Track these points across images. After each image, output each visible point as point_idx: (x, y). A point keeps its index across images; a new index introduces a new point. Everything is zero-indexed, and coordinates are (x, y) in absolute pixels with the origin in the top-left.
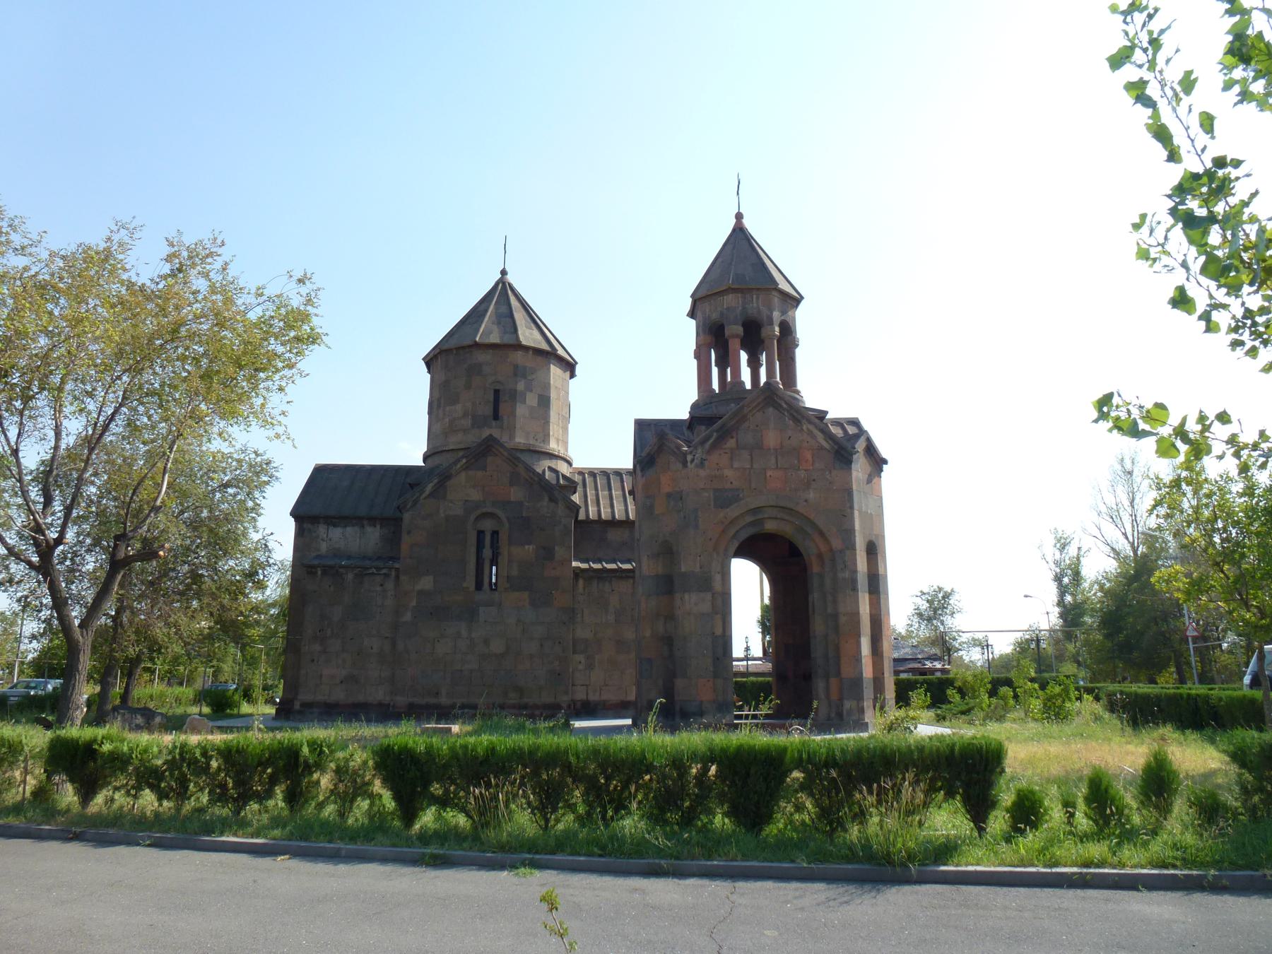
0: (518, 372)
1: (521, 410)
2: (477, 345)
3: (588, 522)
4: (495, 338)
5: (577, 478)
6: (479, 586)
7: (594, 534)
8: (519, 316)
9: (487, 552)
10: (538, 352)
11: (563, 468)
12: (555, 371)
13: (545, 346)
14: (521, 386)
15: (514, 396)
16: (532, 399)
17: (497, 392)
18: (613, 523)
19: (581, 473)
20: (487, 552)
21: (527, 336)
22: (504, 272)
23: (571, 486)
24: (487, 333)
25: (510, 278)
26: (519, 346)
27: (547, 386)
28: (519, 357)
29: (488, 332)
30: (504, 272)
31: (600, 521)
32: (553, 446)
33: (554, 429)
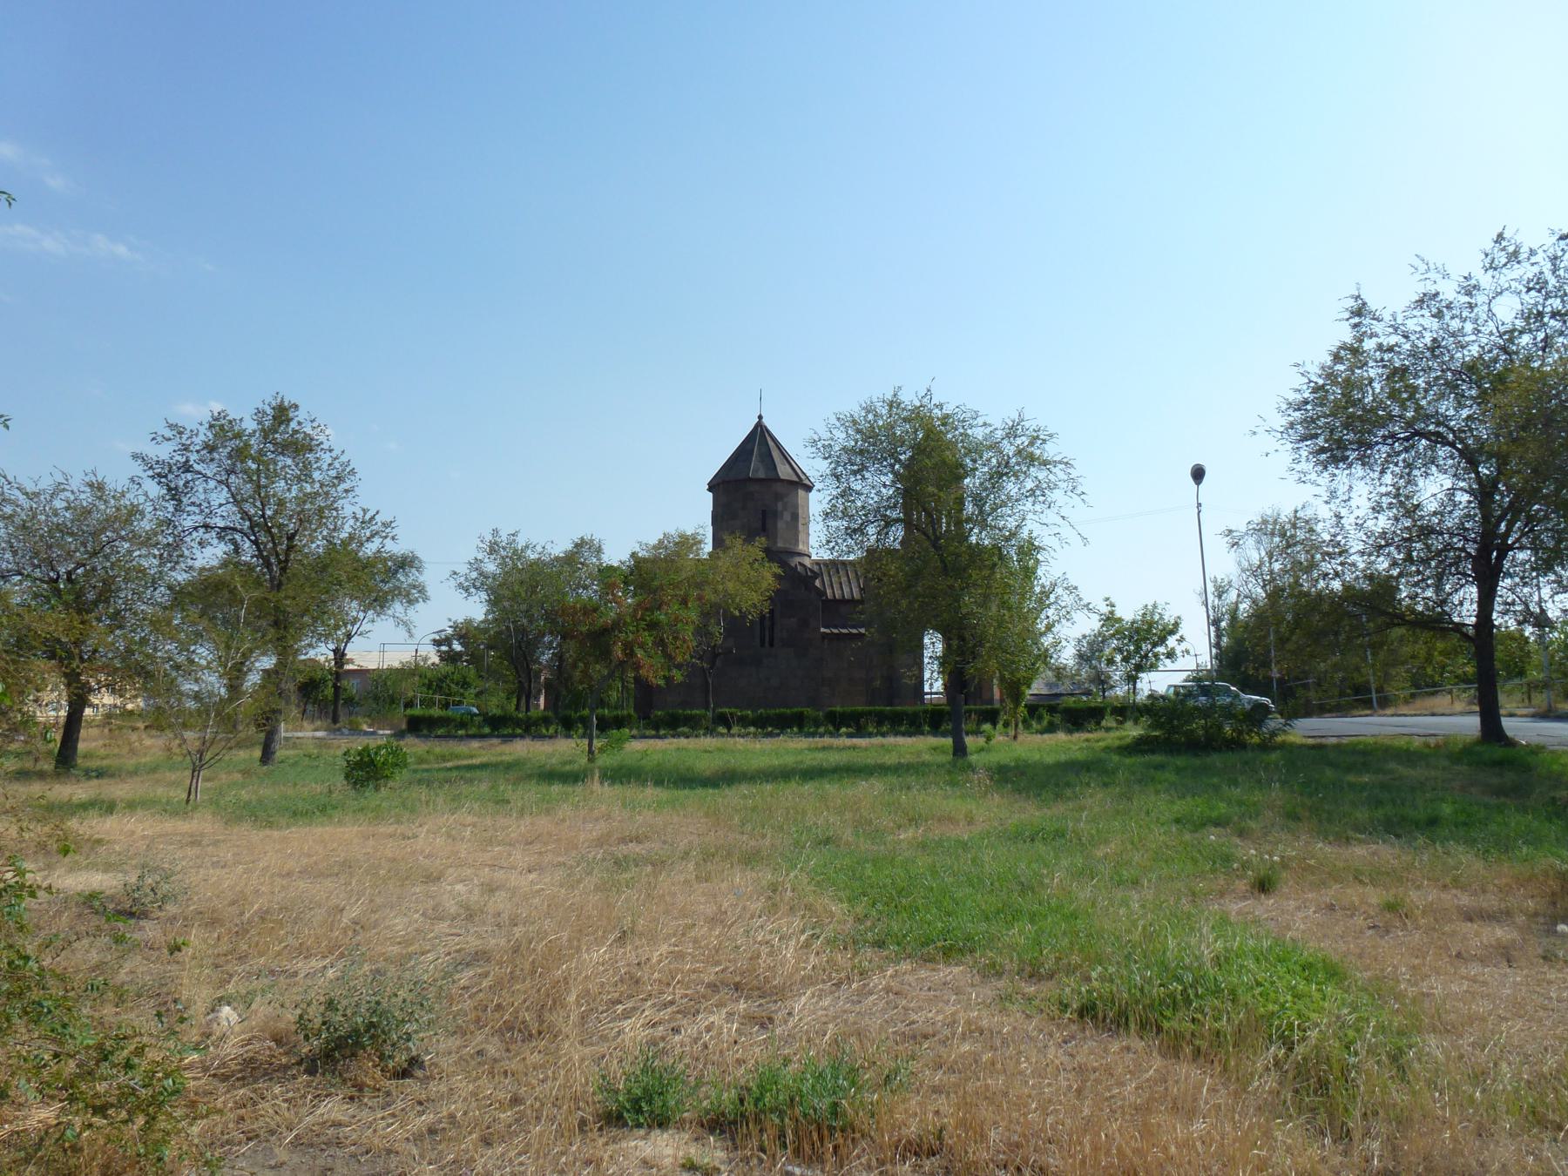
0: (778, 497)
1: (781, 525)
2: (750, 479)
3: (827, 600)
4: (761, 474)
5: (816, 568)
6: (762, 645)
7: (836, 609)
8: (775, 454)
9: (767, 623)
10: (791, 482)
11: (807, 562)
12: (801, 493)
13: (795, 478)
14: (780, 506)
15: (776, 515)
16: (787, 516)
17: (764, 512)
18: (843, 601)
19: (817, 563)
20: (767, 623)
21: (784, 472)
22: (760, 417)
23: (816, 575)
24: (756, 471)
25: (765, 421)
26: (779, 480)
27: (796, 506)
28: (778, 487)
29: (756, 469)
30: (760, 417)
31: (835, 600)
32: (801, 547)
33: (801, 537)
